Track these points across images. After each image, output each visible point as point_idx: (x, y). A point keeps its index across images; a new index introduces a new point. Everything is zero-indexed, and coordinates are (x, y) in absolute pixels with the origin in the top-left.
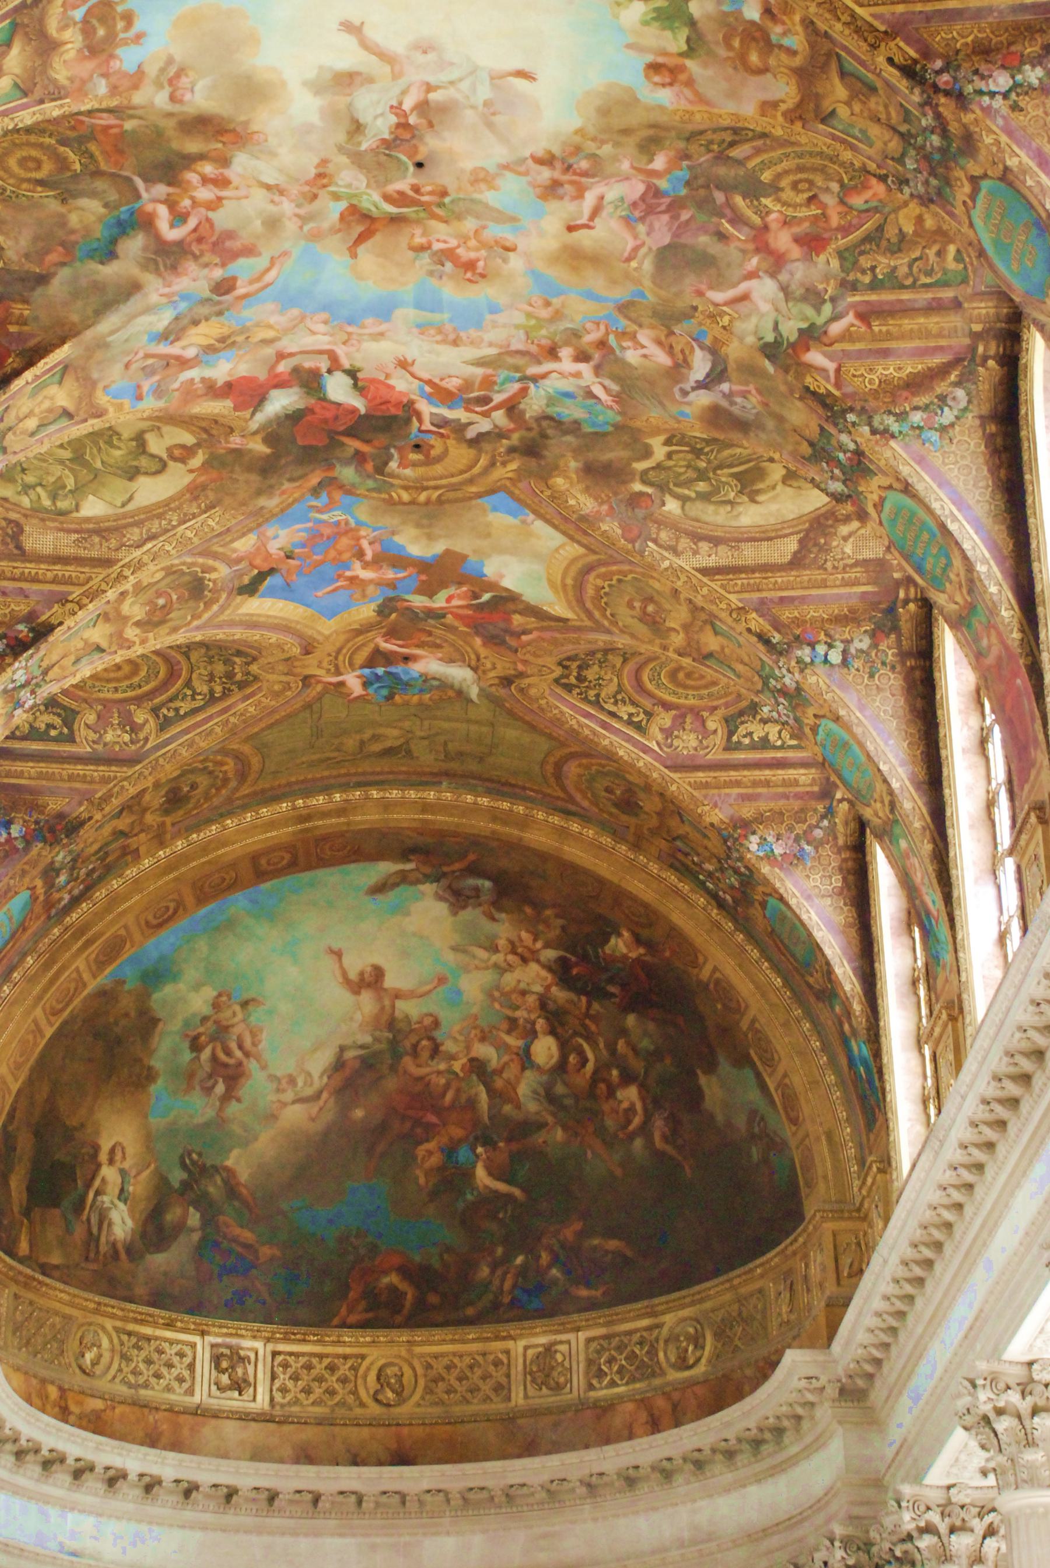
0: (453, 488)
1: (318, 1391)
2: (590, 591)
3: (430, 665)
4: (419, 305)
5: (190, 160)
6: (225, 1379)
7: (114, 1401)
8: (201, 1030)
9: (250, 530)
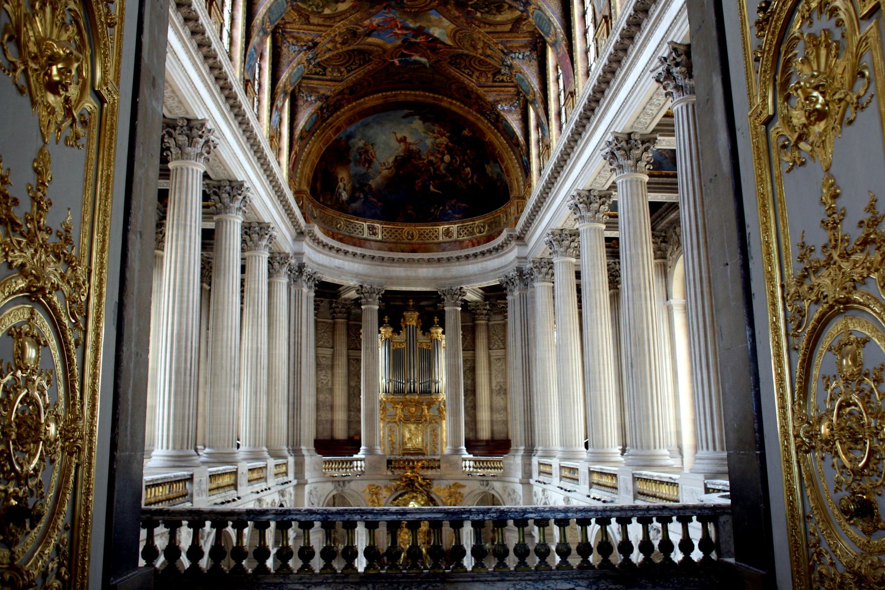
0: (421, 8)
2: (457, 38)
3: (416, 57)
7: (345, 236)
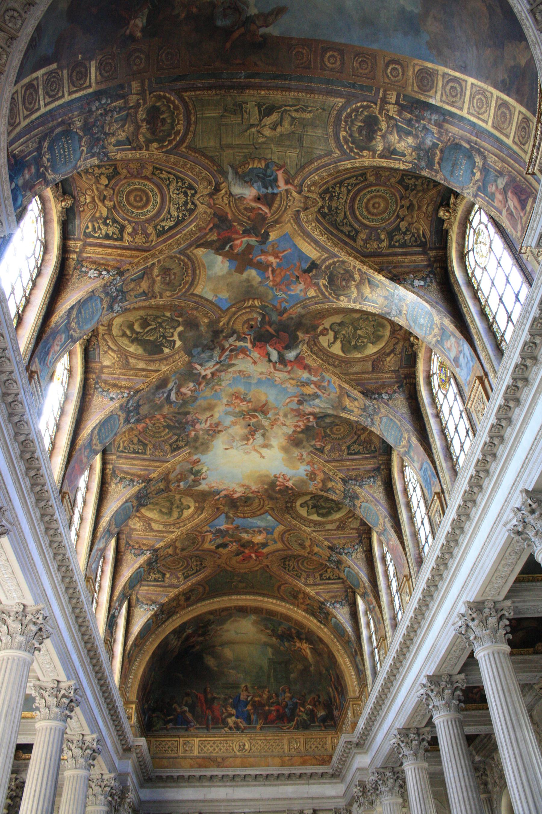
0: (240, 309)
3: (249, 193)
4: (250, 384)
5: (302, 432)
9: (309, 299)
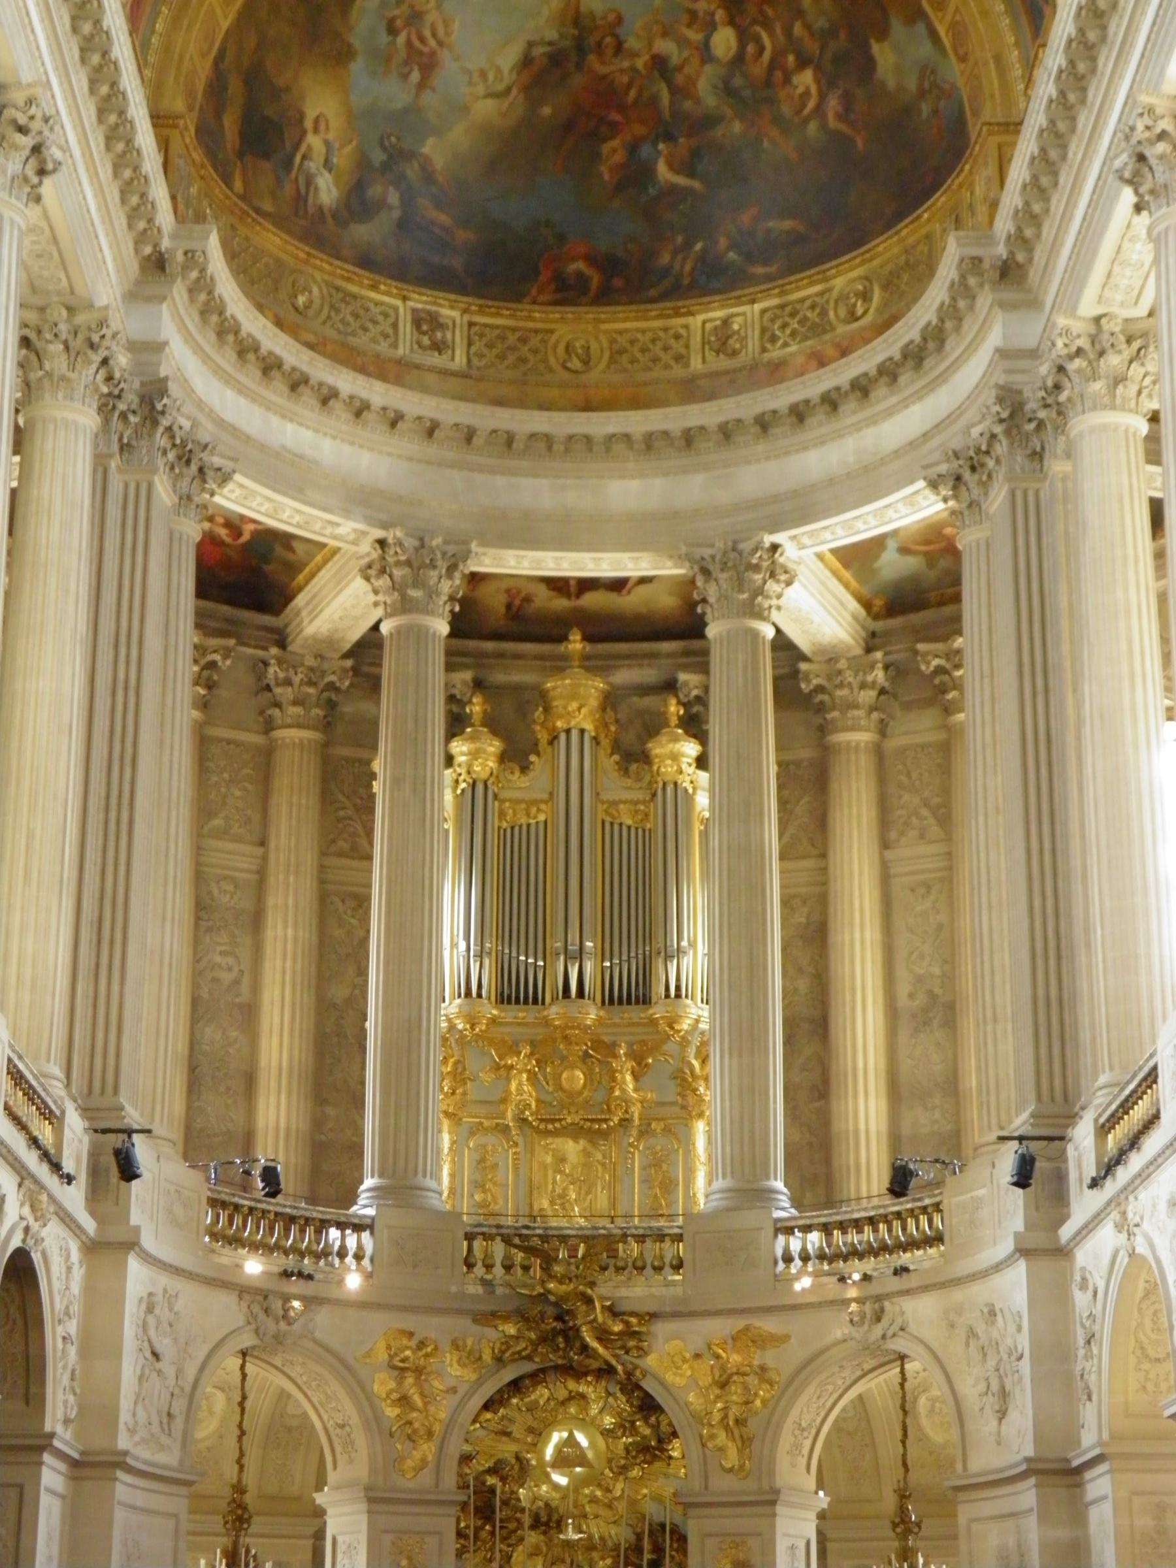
1: (511, 358)
6: (426, 341)
8: (397, 12)
